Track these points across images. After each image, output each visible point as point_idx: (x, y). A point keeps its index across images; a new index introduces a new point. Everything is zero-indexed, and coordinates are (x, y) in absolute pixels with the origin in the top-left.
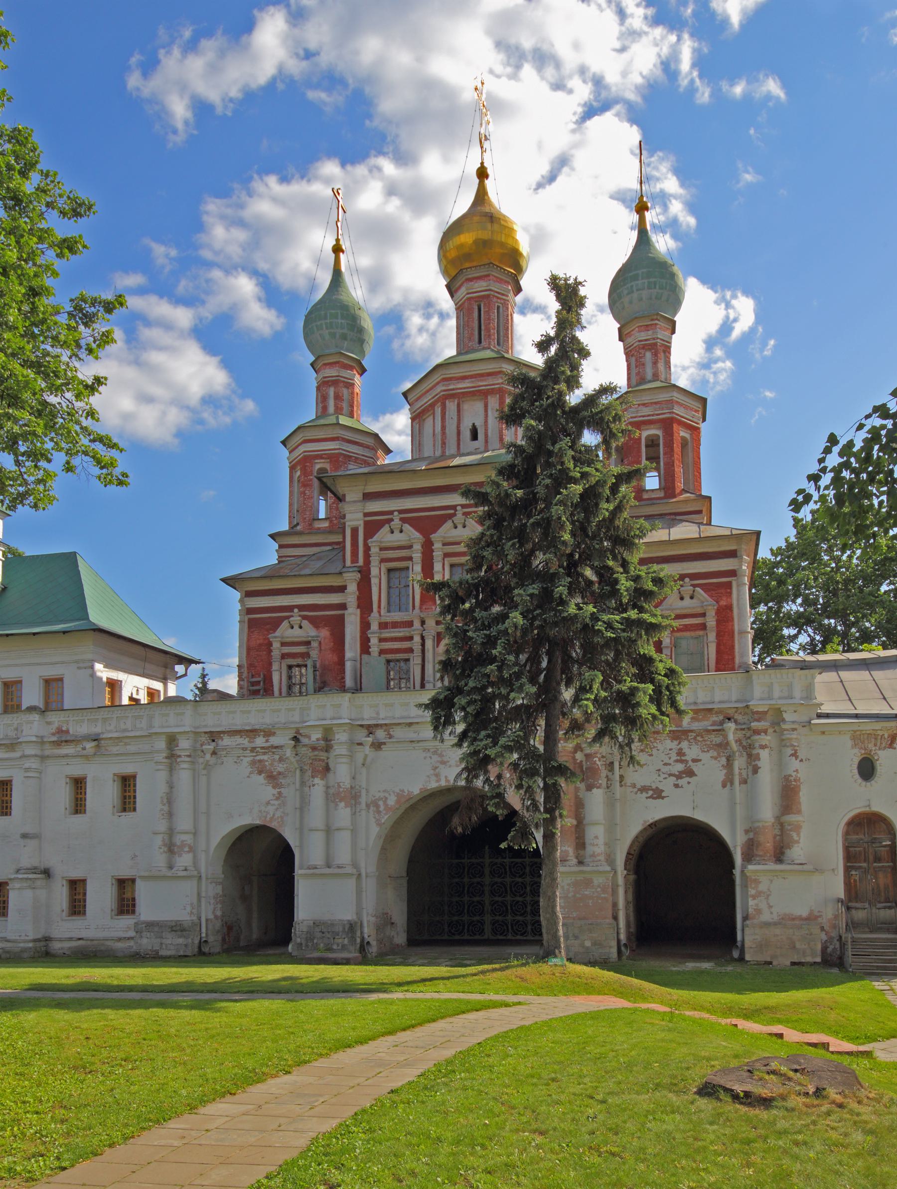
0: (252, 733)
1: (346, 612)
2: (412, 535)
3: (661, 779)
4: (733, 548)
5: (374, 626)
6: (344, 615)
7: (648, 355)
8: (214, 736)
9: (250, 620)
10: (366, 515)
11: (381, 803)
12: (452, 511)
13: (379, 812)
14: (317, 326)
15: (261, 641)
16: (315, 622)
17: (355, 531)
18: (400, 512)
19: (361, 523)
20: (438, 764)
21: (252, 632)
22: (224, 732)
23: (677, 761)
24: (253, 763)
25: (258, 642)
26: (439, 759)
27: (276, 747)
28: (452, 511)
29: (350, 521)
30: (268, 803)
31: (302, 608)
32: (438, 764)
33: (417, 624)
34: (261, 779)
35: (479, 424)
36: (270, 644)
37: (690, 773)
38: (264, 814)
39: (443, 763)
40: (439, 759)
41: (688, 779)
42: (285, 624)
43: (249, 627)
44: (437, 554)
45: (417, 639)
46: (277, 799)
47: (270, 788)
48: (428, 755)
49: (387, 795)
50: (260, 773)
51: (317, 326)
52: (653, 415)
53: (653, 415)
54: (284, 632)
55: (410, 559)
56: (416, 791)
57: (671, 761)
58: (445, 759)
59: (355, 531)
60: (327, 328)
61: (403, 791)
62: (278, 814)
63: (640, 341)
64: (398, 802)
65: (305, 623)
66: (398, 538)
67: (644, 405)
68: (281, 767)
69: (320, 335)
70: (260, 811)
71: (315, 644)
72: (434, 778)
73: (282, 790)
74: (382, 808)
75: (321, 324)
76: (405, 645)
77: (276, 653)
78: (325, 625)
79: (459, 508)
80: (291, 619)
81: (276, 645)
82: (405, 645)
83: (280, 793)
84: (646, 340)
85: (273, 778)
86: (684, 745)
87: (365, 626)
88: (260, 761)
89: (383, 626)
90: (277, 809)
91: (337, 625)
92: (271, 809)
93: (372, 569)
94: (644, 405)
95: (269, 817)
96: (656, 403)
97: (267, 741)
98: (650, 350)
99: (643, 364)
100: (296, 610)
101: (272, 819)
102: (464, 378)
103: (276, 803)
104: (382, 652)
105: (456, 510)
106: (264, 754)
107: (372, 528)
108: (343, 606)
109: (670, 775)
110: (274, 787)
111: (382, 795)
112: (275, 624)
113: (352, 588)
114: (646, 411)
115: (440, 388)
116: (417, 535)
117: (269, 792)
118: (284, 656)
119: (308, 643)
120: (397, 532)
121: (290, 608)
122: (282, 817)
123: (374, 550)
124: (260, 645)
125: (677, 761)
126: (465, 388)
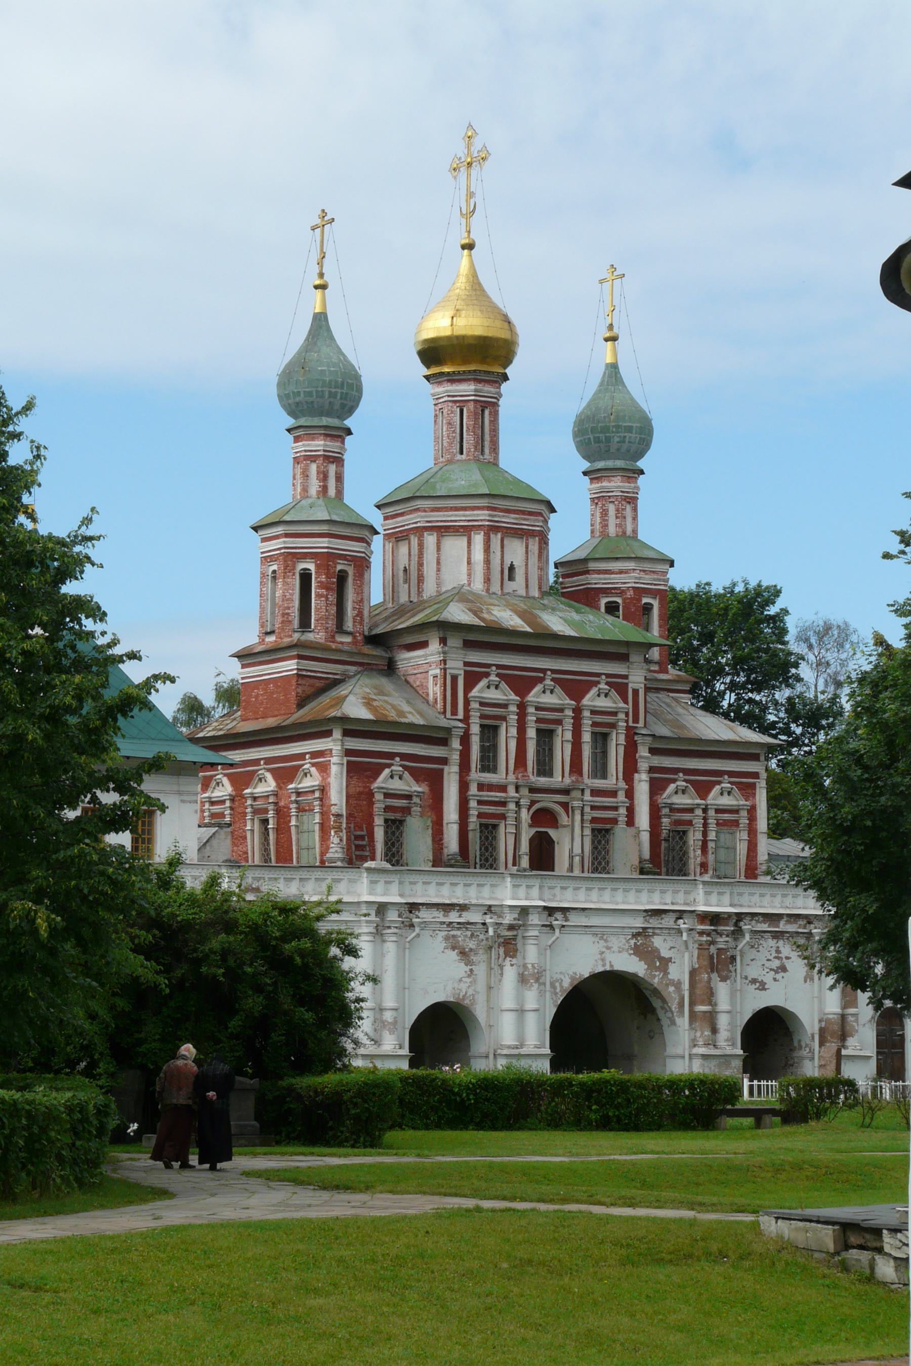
0: (447, 907)
1: (446, 768)
2: (503, 694)
3: (764, 972)
4: (757, 752)
5: (473, 790)
6: (442, 770)
7: (629, 508)
8: (413, 907)
9: (348, 762)
10: (466, 664)
11: (557, 984)
12: (542, 675)
13: (556, 994)
14: (330, 392)
15: (361, 789)
16: (417, 775)
17: (454, 679)
18: (499, 667)
19: (462, 672)
20: (604, 950)
21: (351, 777)
22: (423, 904)
23: (775, 957)
24: (447, 938)
25: (358, 789)
26: (605, 944)
27: (472, 923)
28: (542, 675)
30: (460, 980)
31: (404, 757)
32: (604, 950)
34: (454, 955)
35: (519, 562)
36: (371, 794)
37: (783, 969)
38: (458, 991)
39: (608, 948)
40: (605, 944)
41: (782, 974)
42: (387, 771)
43: (348, 772)
44: (531, 719)
45: (512, 806)
46: (469, 976)
47: (462, 965)
48: (597, 939)
49: (562, 977)
50: (453, 948)
52: (651, 584)
53: (651, 584)
54: (382, 781)
55: (504, 718)
56: (587, 975)
57: (771, 958)
58: (610, 944)
59: (454, 679)
60: (341, 398)
61: (575, 973)
62: (470, 992)
63: (622, 492)
64: (571, 984)
65: (406, 775)
66: (493, 695)
67: (644, 571)
68: (472, 944)
70: (454, 988)
71: (416, 800)
72: (600, 963)
73: (473, 967)
74: (558, 990)
76: (500, 810)
77: (378, 807)
78: (425, 780)
79: (549, 673)
80: (393, 768)
81: (379, 797)
82: (500, 810)
83: (471, 970)
84: (627, 492)
85: (464, 954)
86: (781, 943)
87: (464, 786)
88: (454, 936)
89: (481, 787)
90: (469, 987)
91: (435, 781)
92: (464, 986)
93: (472, 725)
94: (644, 571)
95: (461, 995)
96: (653, 572)
97: (460, 916)
98: (629, 503)
99: (625, 518)
100: (398, 759)
101: (464, 996)
102: (508, 511)
103: (468, 980)
104: (480, 815)
105: (545, 674)
106: (459, 929)
107: (472, 679)
108: (444, 761)
109: (771, 970)
110: (466, 965)
111: (558, 976)
112: (376, 771)
113: (456, 744)
114: (648, 578)
116: (513, 697)
117: (462, 969)
118: (387, 809)
119: (408, 797)
120: (492, 688)
121: (391, 756)
122: (473, 995)
123: (474, 705)
124: (360, 793)
125: (775, 957)
126: (508, 523)
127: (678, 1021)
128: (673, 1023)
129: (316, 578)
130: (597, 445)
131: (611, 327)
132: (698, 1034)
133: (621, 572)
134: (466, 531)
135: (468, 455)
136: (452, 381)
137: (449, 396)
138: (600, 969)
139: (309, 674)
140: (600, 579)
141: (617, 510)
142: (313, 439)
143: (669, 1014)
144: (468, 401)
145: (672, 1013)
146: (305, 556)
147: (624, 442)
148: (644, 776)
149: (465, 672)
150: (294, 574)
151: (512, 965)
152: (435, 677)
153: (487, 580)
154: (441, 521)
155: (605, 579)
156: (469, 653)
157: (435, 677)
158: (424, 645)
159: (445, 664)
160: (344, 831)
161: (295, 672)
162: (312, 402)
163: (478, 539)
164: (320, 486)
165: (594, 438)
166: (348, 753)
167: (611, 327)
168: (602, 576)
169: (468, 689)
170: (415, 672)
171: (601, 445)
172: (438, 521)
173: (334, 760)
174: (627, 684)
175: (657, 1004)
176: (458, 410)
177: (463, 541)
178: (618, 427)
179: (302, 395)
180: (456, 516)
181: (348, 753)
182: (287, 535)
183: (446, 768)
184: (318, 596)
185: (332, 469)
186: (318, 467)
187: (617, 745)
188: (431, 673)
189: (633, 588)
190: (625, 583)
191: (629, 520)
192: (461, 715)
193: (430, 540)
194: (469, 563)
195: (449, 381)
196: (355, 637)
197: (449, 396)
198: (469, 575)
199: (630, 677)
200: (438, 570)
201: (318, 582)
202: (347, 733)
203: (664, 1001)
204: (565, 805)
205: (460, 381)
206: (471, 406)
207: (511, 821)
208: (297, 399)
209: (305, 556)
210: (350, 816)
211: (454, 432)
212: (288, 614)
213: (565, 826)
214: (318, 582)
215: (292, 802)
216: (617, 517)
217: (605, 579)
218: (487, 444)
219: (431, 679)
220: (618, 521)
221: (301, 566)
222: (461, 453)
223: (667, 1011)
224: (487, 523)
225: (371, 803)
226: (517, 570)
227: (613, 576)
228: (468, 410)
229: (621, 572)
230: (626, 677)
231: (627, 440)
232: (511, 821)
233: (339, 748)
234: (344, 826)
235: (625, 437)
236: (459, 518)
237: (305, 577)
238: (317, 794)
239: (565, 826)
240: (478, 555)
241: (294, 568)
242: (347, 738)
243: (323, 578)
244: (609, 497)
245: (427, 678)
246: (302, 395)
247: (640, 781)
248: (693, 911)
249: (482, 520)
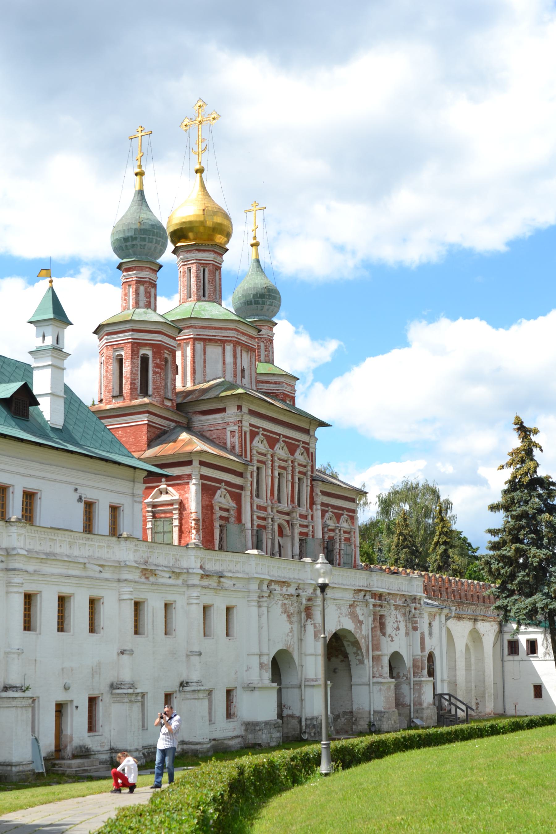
1: (243, 493)
6: (240, 494)
9: (203, 484)
10: (251, 425)
12: (278, 437)
14: (156, 240)
19: (248, 430)
28: (278, 437)
29: (245, 427)
33: (269, 509)
34: (284, 616)
43: (203, 490)
47: (288, 624)
50: (285, 612)
51: (156, 240)
59: (245, 433)
69: (155, 247)
71: (232, 512)
75: (160, 241)
81: (216, 508)
100: (223, 484)
115: (233, 334)
127: (366, 661)
128: (361, 662)
129: (153, 361)
130: (256, 305)
131: (255, 238)
132: (375, 669)
133: (275, 383)
134: (222, 342)
135: (209, 298)
136: (199, 250)
137: (196, 259)
138: (338, 628)
139: (153, 424)
140: (264, 386)
141: (266, 346)
142: (142, 270)
143: (360, 657)
144: (209, 264)
145: (363, 656)
146: (146, 345)
147: (272, 305)
148: (319, 507)
149: (251, 430)
150: (138, 357)
151: (312, 624)
152: (233, 432)
153: (235, 375)
154: (206, 335)
155: (267, 387)
156: (252, 418)
157: (233, 432)
158: (223, 410)
159: (242, 423)
160: (201, 531)
161: (147, 422)
162: (145, 245)
163: (229, 348)
164: (147, 302)
165: (255, 301)
166: (203, 477)
167: (255, 238)
168: (265, 385)
169: (251, 442)
170: (212, 429)
171: (259, 306)
172: (204, 335)
173: (194, 481)
174: (309, 448)
175: (350, 650)
176: (202, 269)
177: (220, 349)
178: (270, 295)
179: (138, 240)
180: (216, 332)
181: (203, 477)
182: (133, 330)
183: (243, 493)
184: (155, 373)
185: (153, 290)
186: (145, 289)
187: (307, 486)
188: (228, 429)
189: (283, 393)
190: (278, 390)
191: (271, 353)
192: (248, 459)
193: (199, 346)
194: (224, 363)
195: (197, 250)
196: (173, 403)
197: (196, 259)
198: (224, 371)
199: (311, 445)
200: (205, 366)
201: (155, 363)
202: (202, 463)
203: (359, 648)
204: (288, 522)
205: (204, 251)
206: (211, 267)
207: (269, 531)
208: (134, 243)
209: (146, 345)
210: (203, 520)
211: (200, 282)
212: (134, 383)
213: (287, 536)
214: (155, 363)
215: (148, 512)
216: (266, 351)
217: (267, 387)
218: (218, 292)
219: (228, 434)
220: (266, 353)
221: (142, 352)
222: (204, 296)
223: (358, 655)
224: (235, 339)
225: (212, 513)
226: (246, 372)
227: (271, 385)
228: (209, 270)
229: (275, 383)
230: (308, 444)
231: (273, 304)
232: (269, 531)
233: (197, 473)
234: (201, 528)
235: (273, 302)
236: (219, 334)
237: (145, 360)
238: (177, 506)
239: (287, 536)
240: (229, 359)
241: (138, 353)
242: (202, 467)
243: (158, 361)
244: (261, 338)
245: (226, 432)
246: (138, 240)
247: (317, 510)
248: (370, 591)
249: (232, 337)
